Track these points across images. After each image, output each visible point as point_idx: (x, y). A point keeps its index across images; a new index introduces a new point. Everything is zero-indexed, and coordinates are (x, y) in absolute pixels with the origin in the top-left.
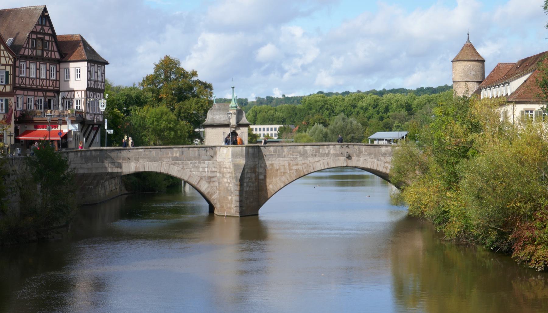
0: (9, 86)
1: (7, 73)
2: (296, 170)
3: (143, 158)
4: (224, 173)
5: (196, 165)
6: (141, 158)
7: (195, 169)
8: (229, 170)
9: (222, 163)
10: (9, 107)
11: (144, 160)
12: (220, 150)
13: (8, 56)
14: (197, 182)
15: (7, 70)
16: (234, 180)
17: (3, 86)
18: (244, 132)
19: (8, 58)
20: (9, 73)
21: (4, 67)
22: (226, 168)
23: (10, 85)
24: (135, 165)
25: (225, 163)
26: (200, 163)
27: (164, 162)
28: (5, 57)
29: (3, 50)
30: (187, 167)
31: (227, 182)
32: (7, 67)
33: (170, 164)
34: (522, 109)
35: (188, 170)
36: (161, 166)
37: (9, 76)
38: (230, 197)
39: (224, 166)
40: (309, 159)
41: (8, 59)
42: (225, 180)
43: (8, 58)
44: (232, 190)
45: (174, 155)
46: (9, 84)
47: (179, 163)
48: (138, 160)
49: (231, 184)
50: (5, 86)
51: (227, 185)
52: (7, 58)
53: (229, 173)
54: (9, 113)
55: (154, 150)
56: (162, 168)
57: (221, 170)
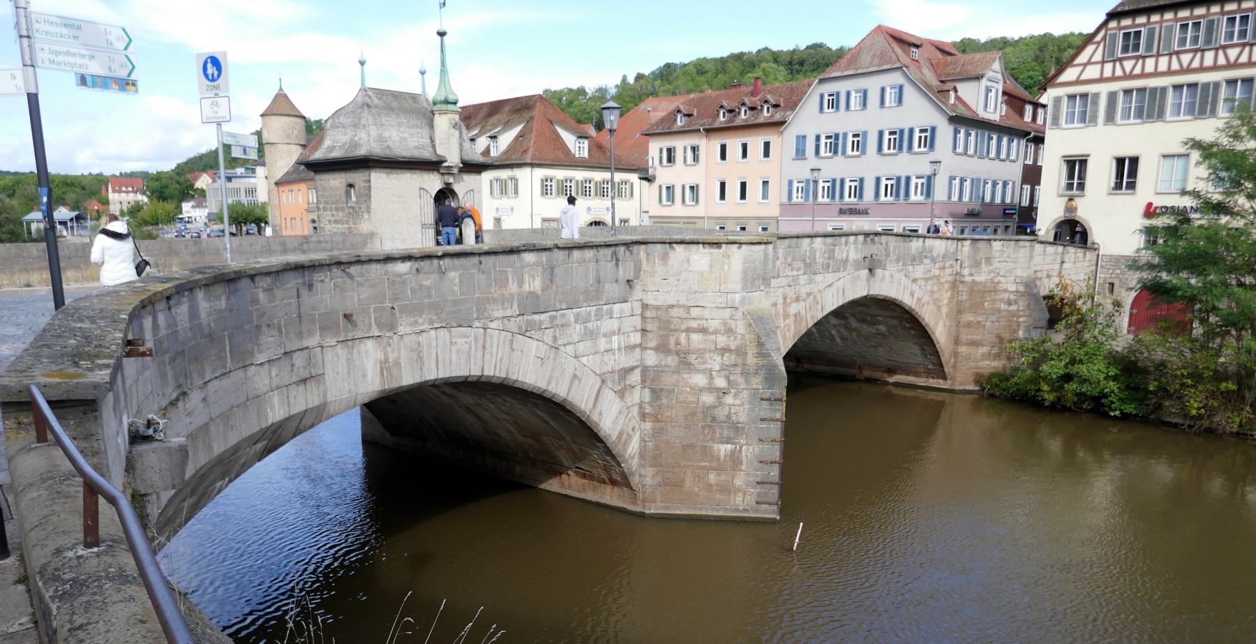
2: (795, 315)
3: (415, 310)
4: (688, 352)
5: (590, 325)
6: (404, 309)
7: (588, 343)
8: (722, 340)
9: (675, 313)
11: (416, 322)
12: (665, 258)
14: (594, 396)
16: (757, 382)
18: (472, 190)
22: (703, 331)
24: (381, 355)
25: (695, 312)
26: (599, 316)
27: (493, 325)
30: (565, 341)
31: (710, 389)
33: (515, 330)
34: (491, 178)
35: (570, 349)
36: (484, 347)
38: (724, 449)
39: (694, 324)
40: (819, 278)
42: (700, 380)
44: (743, 418)
45: (526, 287)
47: (541, 322)
48: (392, 327)
49: (735, 396)
51: (708, 399)
53: (725, 350)
55: (457, 261)
56: (487, 357)
57: (672, 340)
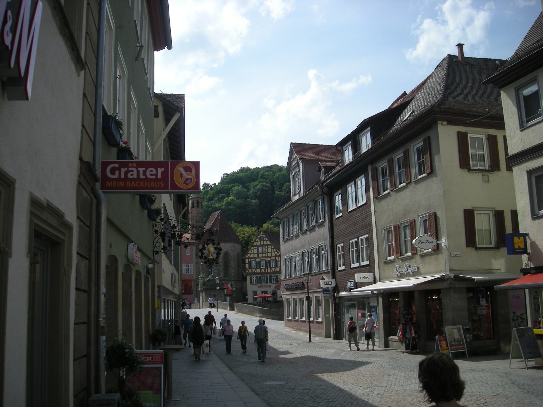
0: (278, 268)
1: (276, 261)
10: (279, 279)
13: (276, 251)
15: (276, 259)
17: (264, 269)
19: (277, 253)
20: (278, 260)
21: (274, 258)
23: (279, 267)
28: (274, 252)
29: (273, 248)
32: (276, 257)
37: (278, 262)
41: (276, 253)
43: (277, 253)
46: (278, 266)
50: (276, 268)
52: (275, 253)
54: (279, 283)
